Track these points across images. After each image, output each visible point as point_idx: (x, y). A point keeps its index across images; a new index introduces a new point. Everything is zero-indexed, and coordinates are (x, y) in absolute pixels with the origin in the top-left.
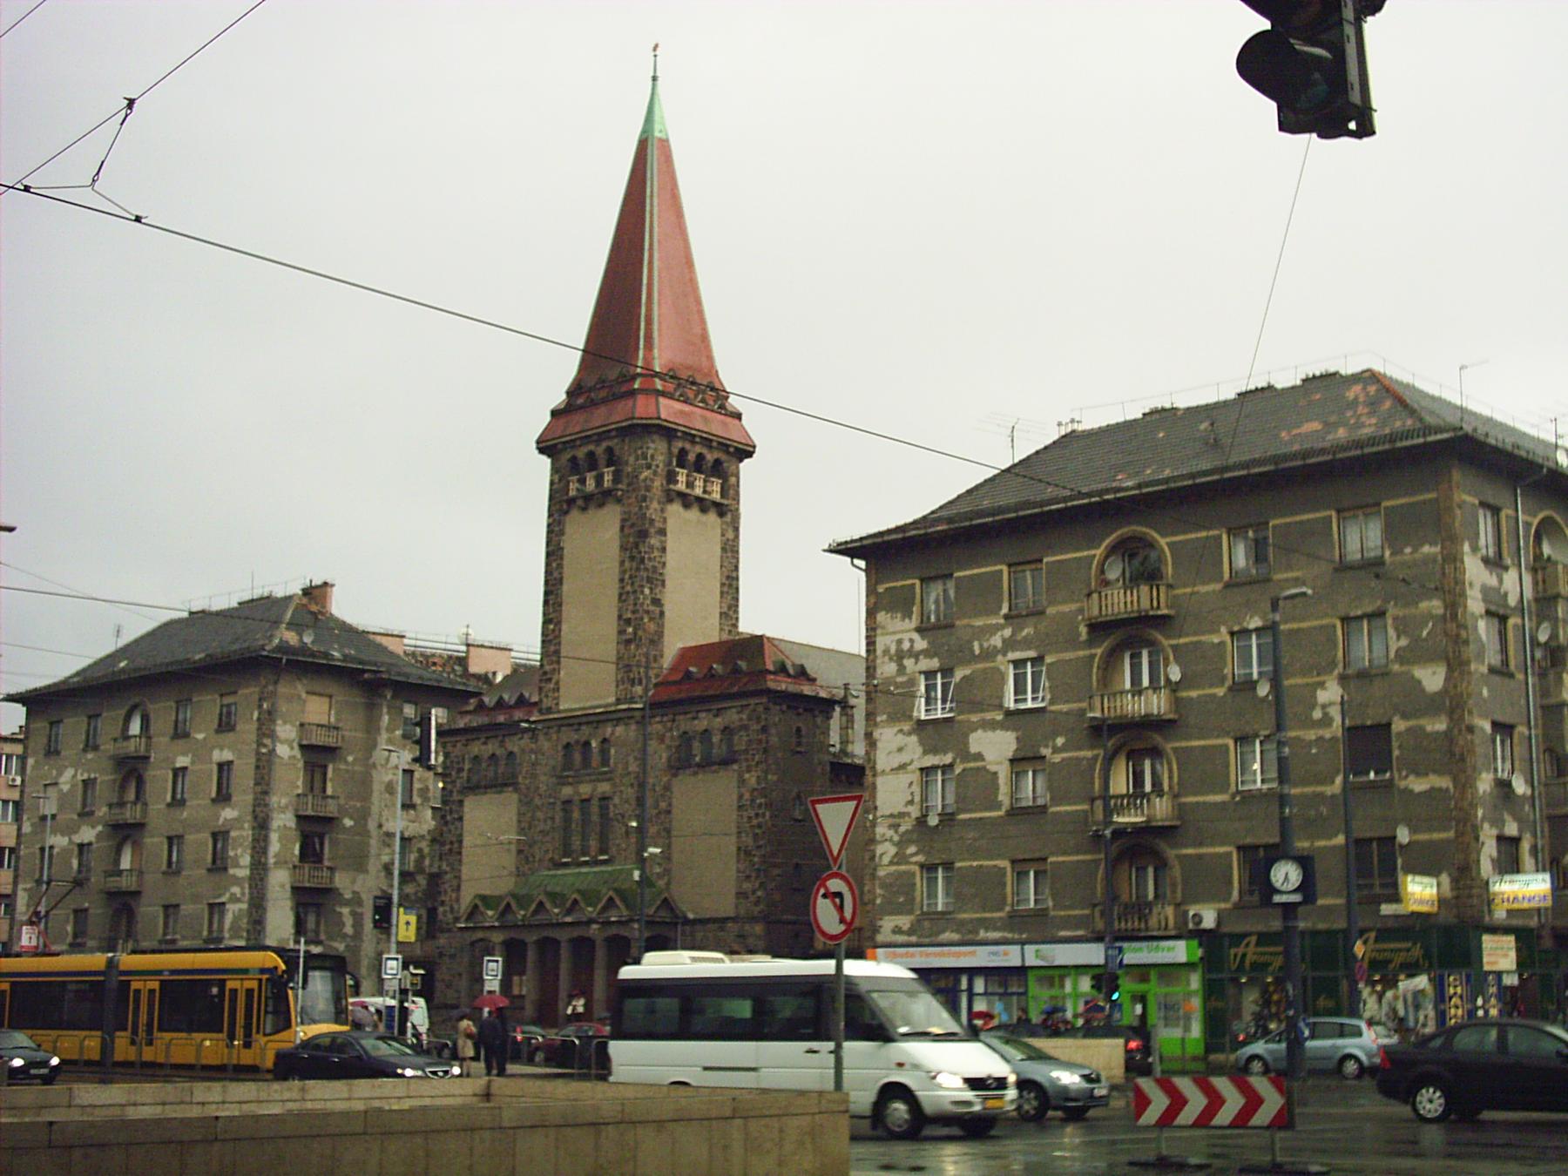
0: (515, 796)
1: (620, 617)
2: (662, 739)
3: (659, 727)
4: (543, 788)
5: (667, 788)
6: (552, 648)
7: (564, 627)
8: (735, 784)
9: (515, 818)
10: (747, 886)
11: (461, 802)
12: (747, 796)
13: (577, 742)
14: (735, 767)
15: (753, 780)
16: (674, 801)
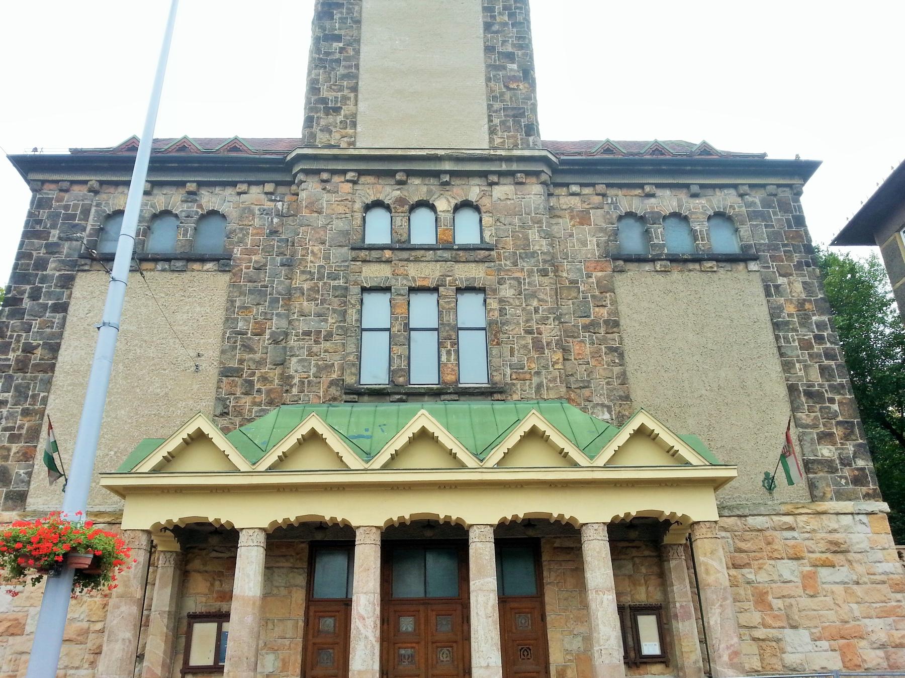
0: (225, 278)
1: (489, 49)
2: (583, 218)
3: (575, 201)
4: (313, 264)
5: (607, 288)
6: (342, 71)
7: (364, 49)
8: (760, 290)
9: (219, 316)
10: (826, 451)
11: (67, 282)
12: (790, 309)
13: (401, 201)
14: (753, 266)
15: (798, 287)
16: (622, 308)
